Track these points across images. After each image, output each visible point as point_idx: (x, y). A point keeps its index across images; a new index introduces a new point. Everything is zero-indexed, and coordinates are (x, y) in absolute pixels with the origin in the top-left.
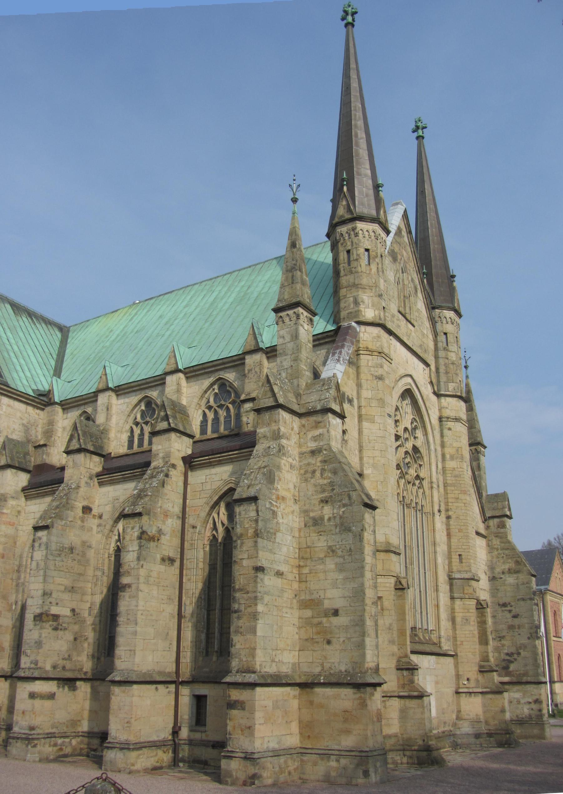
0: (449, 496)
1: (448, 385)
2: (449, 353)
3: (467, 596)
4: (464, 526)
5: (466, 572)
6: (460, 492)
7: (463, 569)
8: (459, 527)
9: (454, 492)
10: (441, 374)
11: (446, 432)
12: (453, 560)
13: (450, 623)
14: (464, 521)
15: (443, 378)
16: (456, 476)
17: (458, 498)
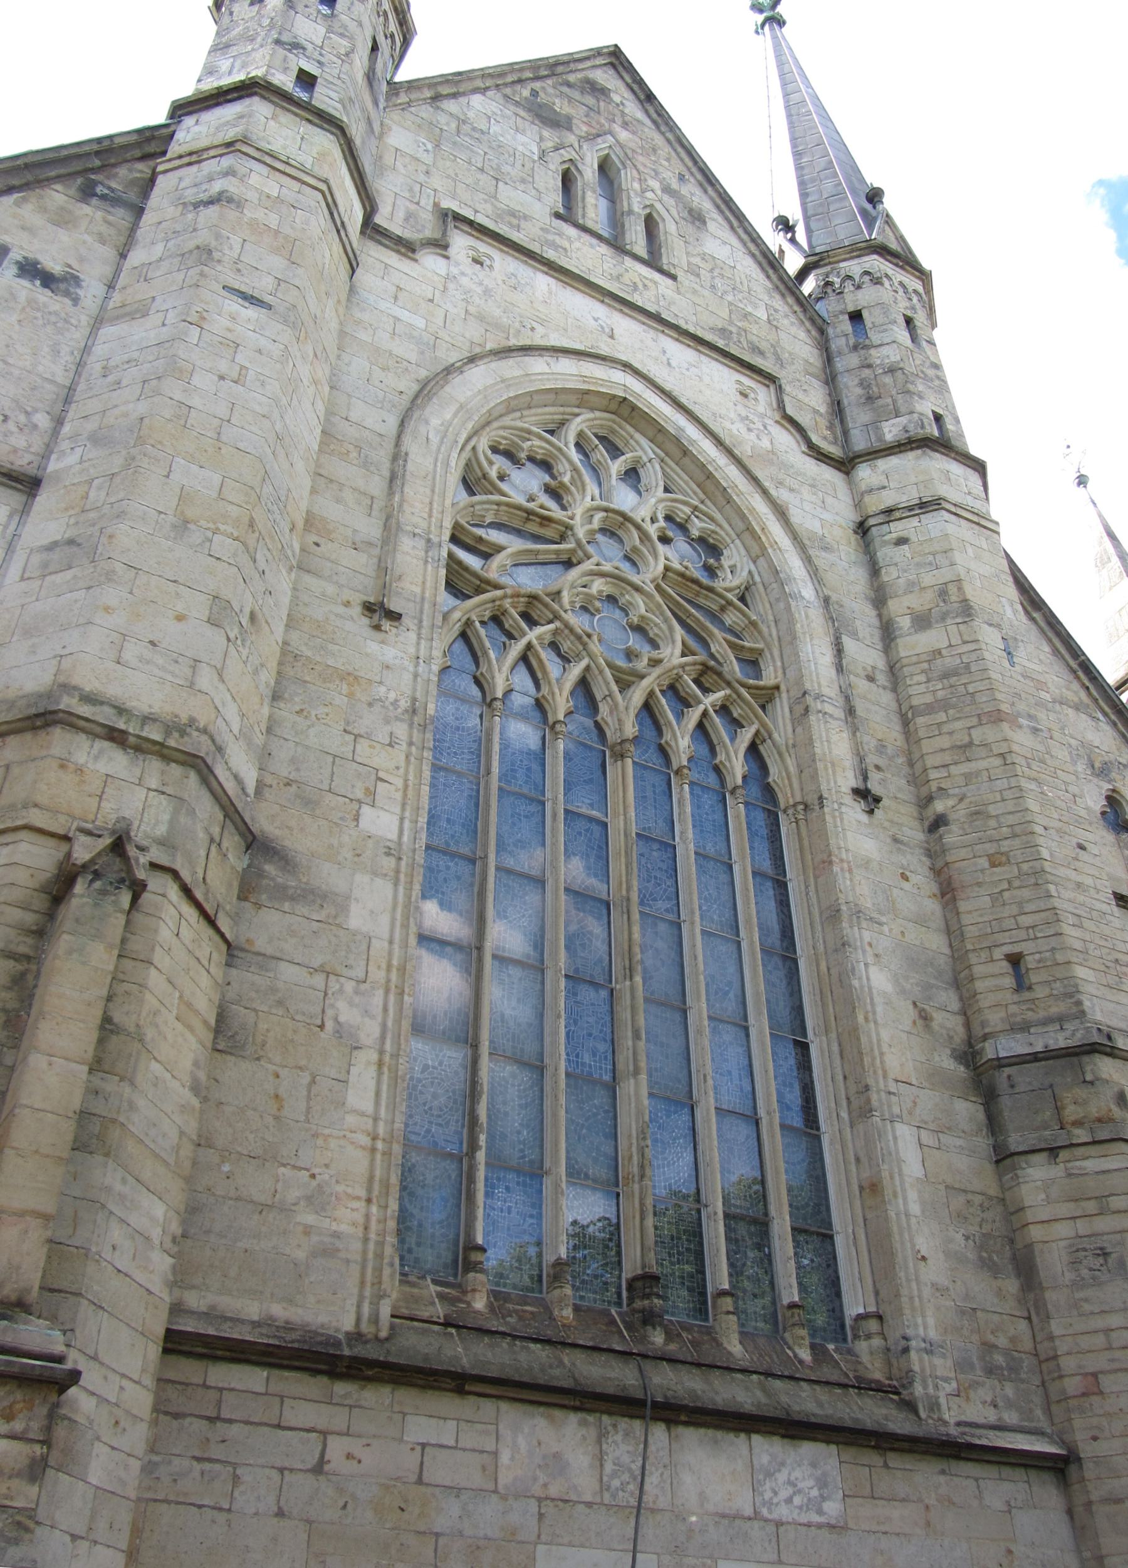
0: (927, 746)
1: (878, 429)
2: (873, 352)
3: (1081, 1135)
4: (1015, 836)
5: (1060, 1020)
6: (975, 721)
7: (1042, 1014)
8: (991, 848)
9: (946, 728)
10: (848, 411)
11: (885, 553)
12: (979, 985)
13: (1012, 1285)
14: (1011, 819)
15: (858, 417)
16: (945, 676)
17: (970, 744)
